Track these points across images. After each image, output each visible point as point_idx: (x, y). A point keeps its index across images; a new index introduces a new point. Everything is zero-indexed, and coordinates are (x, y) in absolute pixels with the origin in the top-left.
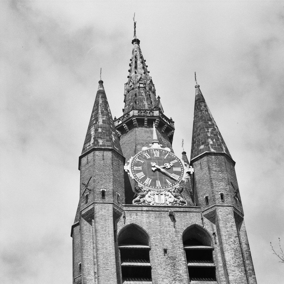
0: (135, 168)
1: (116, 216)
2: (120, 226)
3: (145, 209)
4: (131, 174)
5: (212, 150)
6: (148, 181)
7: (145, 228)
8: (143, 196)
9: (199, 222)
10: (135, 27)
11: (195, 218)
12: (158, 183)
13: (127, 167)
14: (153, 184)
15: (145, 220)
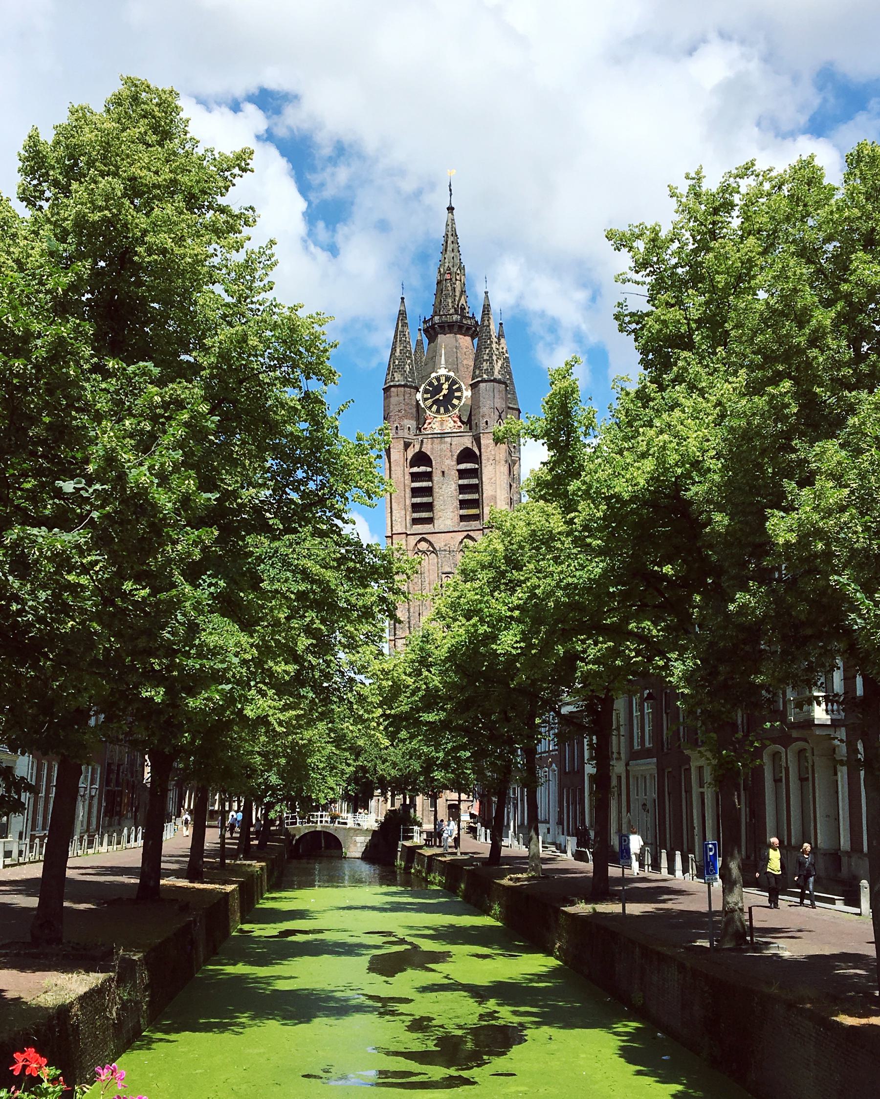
0: (425, 396)
1: (407, 445)
2: (411, 453)
3: (430, 436)
4: (421, 402)
5: (485, 376)
6: (435, 408)
7: (428, 453)
8: (430, 423)
9: (470, 446)
10: (451, 195)
11: (467, 442)
12: (442, 410)
13: (419, 396)
14: (438, 411)
15: (429, 446)
